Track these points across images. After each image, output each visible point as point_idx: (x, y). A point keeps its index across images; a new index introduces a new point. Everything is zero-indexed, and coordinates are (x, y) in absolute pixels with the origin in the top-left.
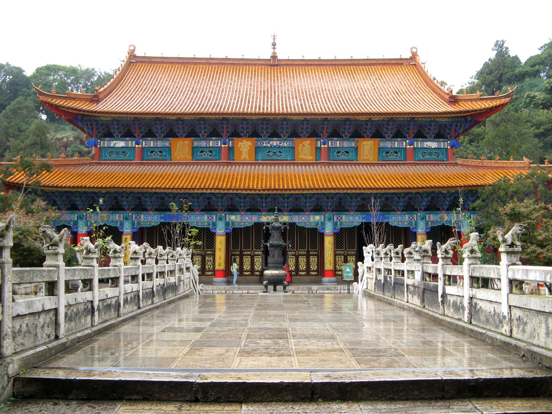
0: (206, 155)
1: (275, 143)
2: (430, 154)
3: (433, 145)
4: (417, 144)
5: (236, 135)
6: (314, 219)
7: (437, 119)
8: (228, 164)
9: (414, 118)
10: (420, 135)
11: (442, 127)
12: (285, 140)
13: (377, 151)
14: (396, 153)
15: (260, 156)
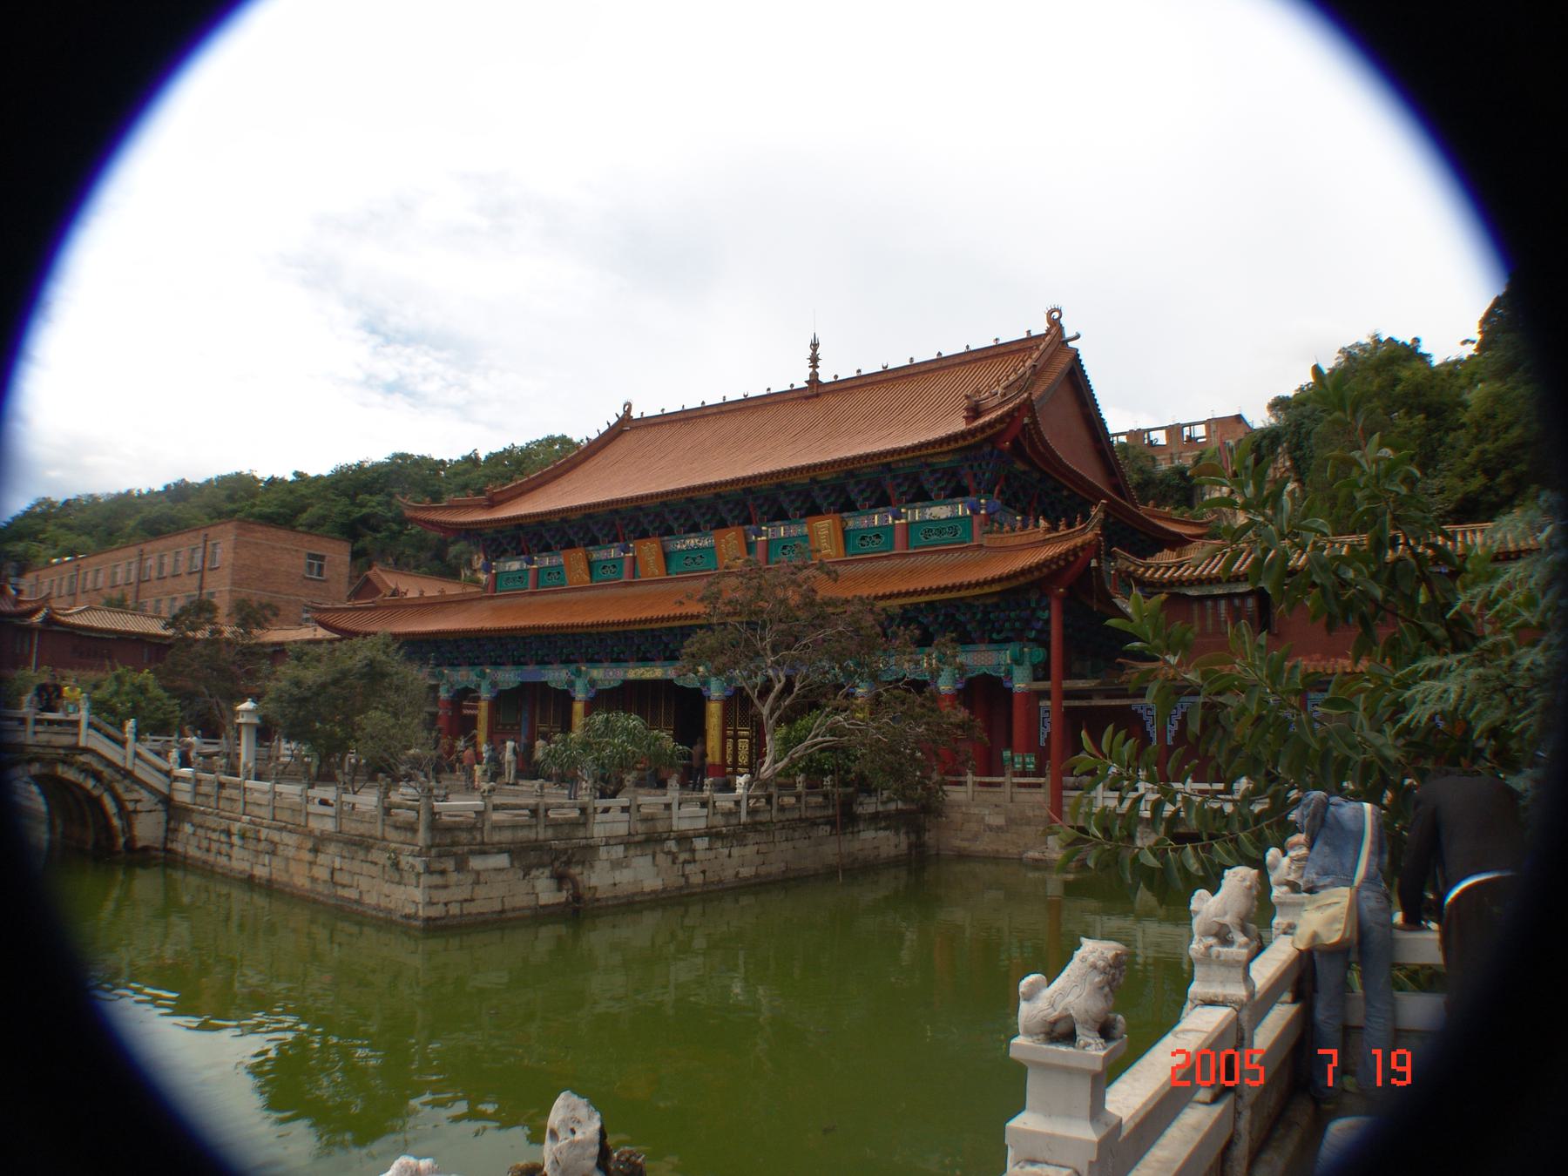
0: (609, 575)
1: (692, 542)
2: (940, 532)
3: (941, 512)
4: (913, 515)
5: (644, 535)
6: (556, 676)
7: (930, 460)
8: (627, 584)
9: (889, 464)
10: (922, 497)
11: (951, 473)
12: (706, 535)
13: (840, 538)
14: (878, 536)
15: (673, 566)
